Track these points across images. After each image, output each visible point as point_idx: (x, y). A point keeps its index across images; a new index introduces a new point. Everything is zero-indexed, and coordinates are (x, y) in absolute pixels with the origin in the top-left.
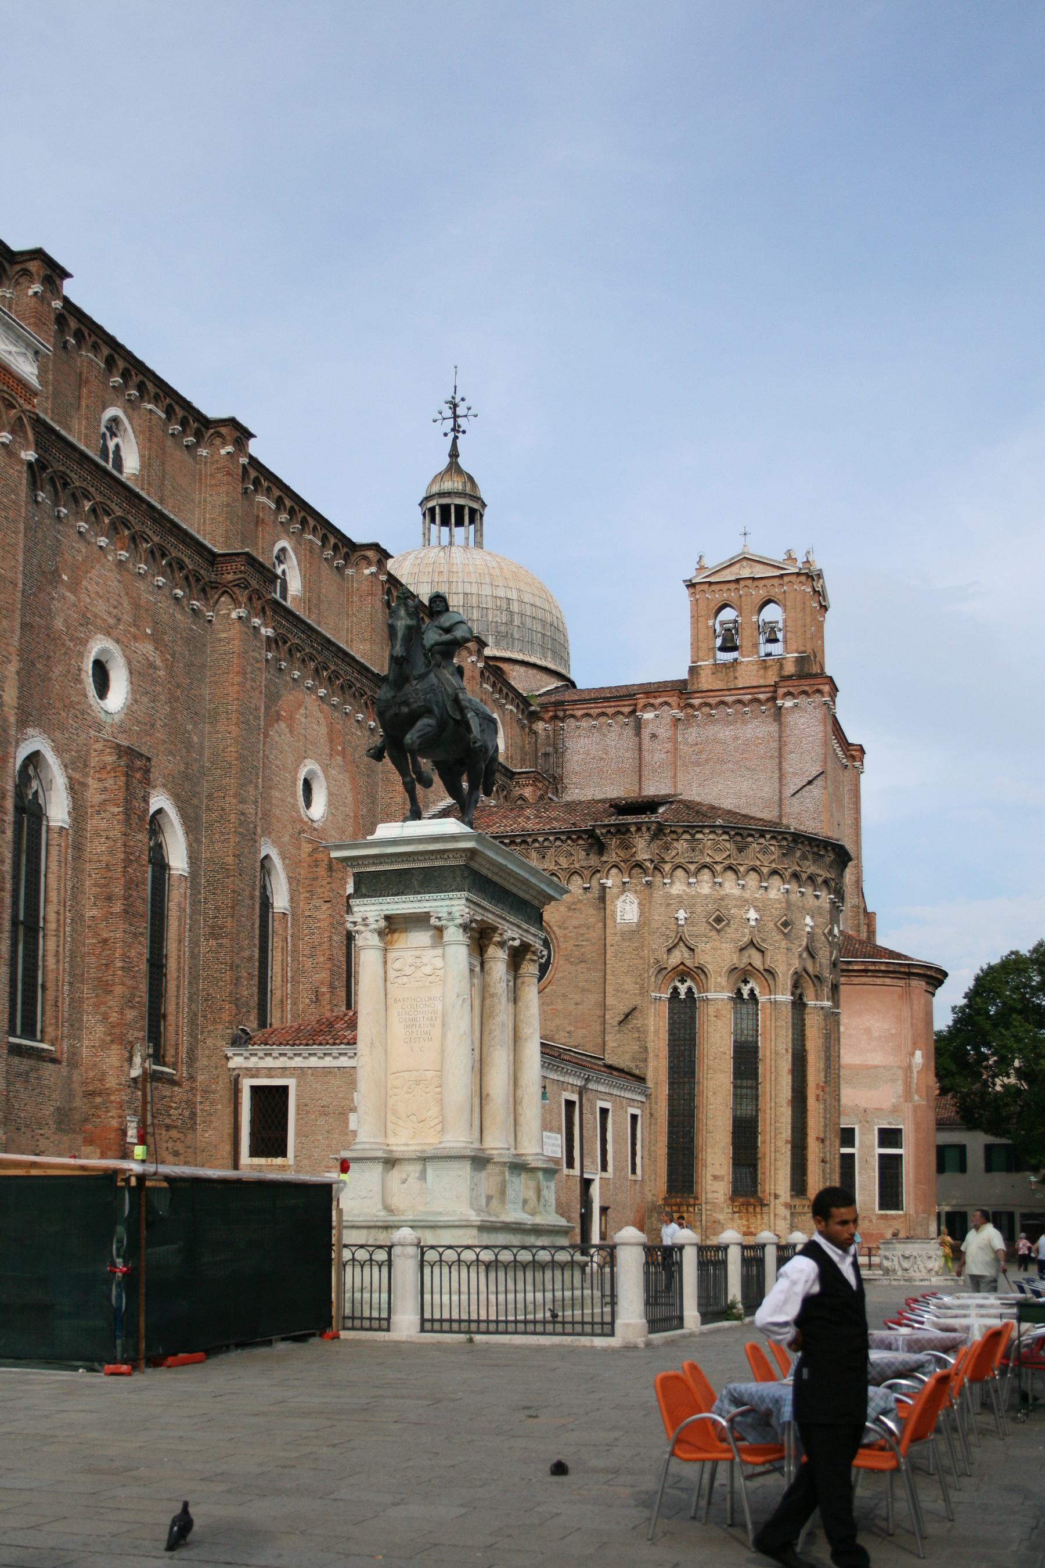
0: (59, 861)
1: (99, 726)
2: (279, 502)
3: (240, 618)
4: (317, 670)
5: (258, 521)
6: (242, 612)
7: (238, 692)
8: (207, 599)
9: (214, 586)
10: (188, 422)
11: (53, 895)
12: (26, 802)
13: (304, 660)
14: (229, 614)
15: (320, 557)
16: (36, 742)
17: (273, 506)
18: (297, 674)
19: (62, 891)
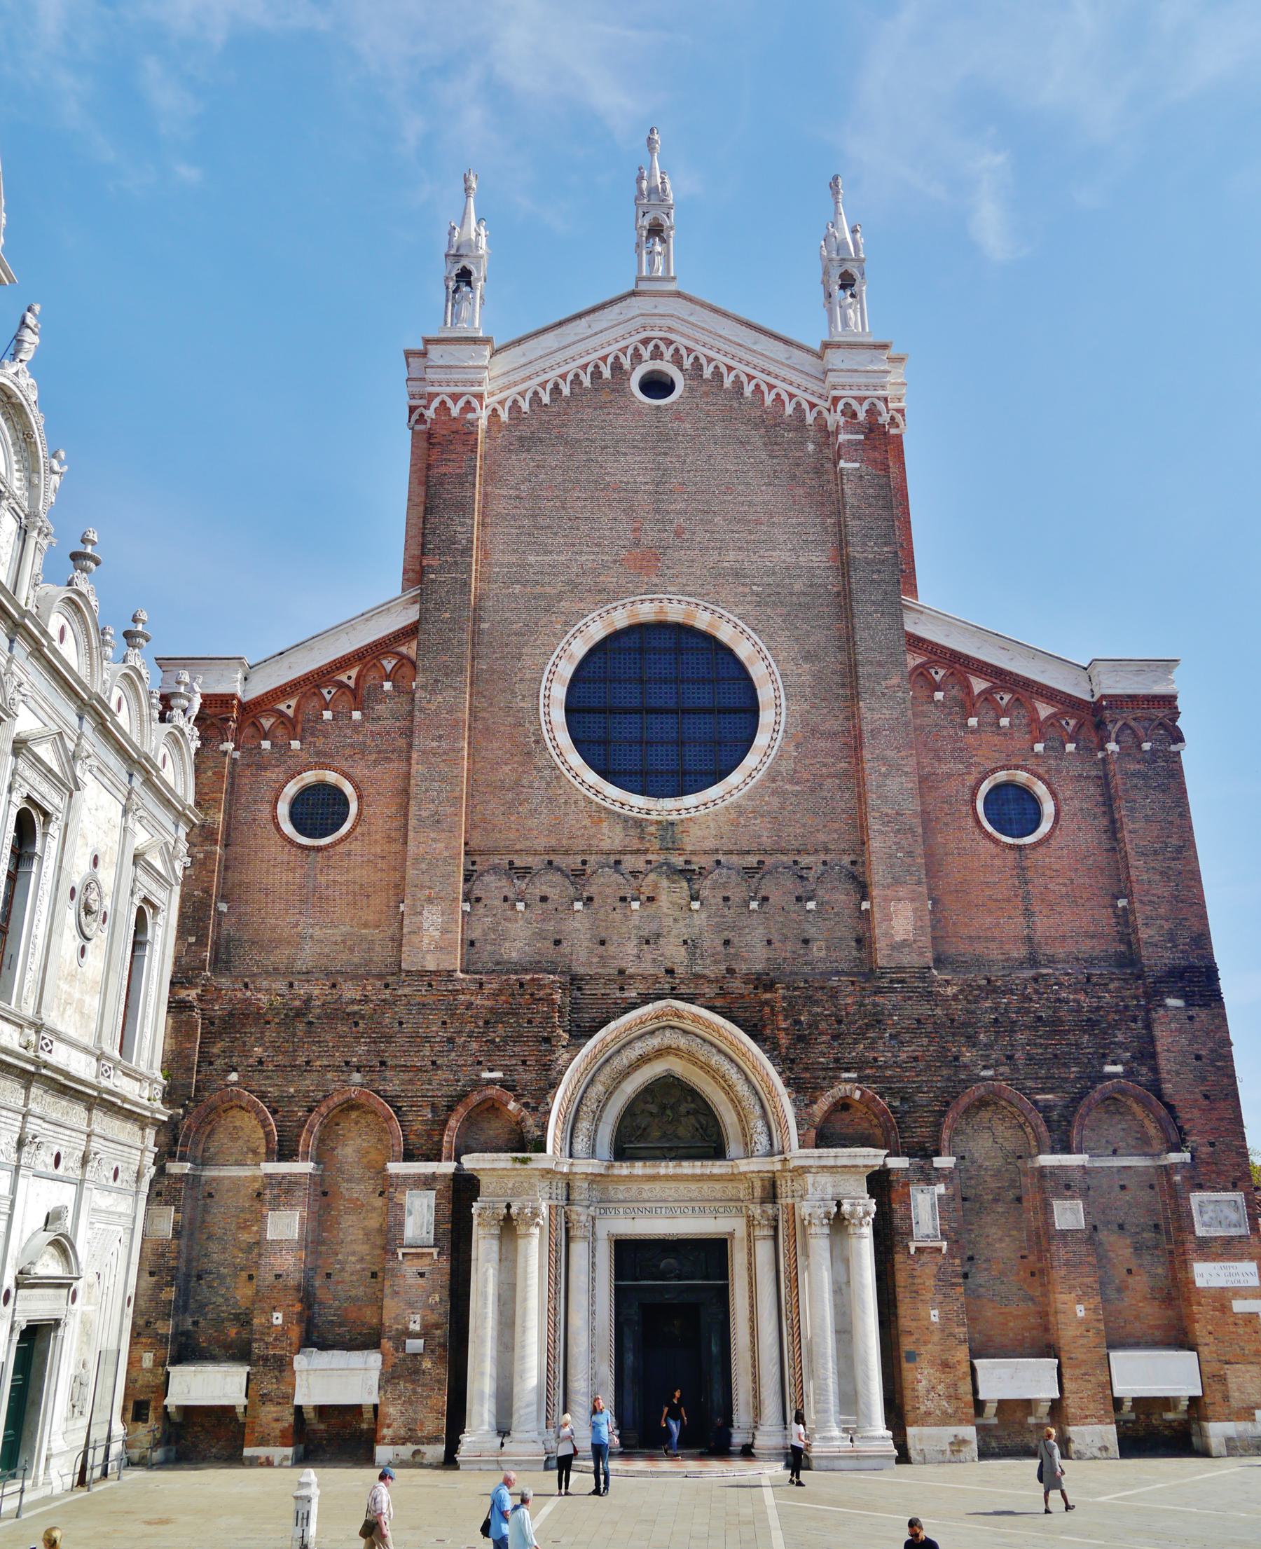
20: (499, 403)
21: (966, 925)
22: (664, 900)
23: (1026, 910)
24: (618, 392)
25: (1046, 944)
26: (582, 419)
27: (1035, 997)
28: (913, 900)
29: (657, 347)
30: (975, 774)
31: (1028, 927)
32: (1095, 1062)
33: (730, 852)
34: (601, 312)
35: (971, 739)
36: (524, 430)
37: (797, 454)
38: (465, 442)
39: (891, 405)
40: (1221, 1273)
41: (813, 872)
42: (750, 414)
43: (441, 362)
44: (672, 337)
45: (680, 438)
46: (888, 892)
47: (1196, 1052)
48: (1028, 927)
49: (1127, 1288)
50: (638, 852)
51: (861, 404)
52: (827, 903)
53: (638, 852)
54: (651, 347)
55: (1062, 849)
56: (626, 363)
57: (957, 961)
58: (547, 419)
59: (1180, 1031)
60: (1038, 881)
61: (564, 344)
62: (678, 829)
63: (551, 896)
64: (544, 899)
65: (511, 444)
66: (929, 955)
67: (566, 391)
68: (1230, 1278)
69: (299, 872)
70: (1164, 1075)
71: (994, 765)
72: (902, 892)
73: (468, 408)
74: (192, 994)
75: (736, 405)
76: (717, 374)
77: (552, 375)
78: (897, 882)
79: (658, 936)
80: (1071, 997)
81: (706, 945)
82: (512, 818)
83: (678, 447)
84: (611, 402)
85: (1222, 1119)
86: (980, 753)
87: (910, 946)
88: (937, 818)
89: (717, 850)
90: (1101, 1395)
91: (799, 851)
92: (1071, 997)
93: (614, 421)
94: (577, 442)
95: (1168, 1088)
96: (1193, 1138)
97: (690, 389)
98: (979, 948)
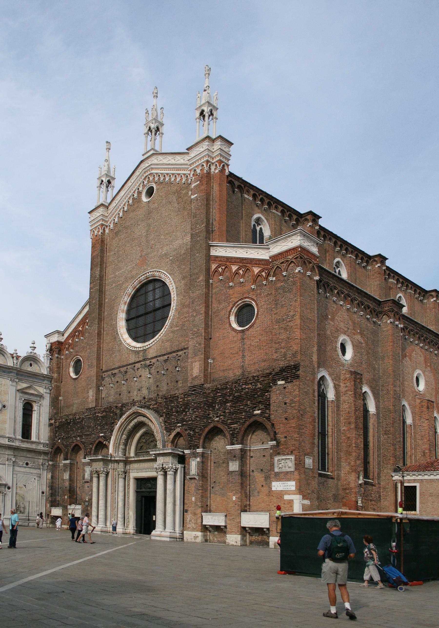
0: (332, 412)
1: (343, 365)
2: (398, 280)
3: (391, 322)
4: (419, 337)
5: (390, 288)
6: (392, 320)
7: (392, 348)
8: (378, 317)
9: (381, 313)
10: (363, 258)
11: (330, 423)
12: (320, 393)
13: (414, 335)
14: (387, 322)
15: (414, 298)
16: (323, 373)
17: (395, 282)
18: (412, 340)
19: (333, 422)
21: (223, 366)
22: (143, 377)
23: (243, 355)
25: (248, 367)
27: (234, 389)
28: (200, 361)
30: (231, 306)
31: (243, 362)
32: (251, 411)
33: (160, 356)
35: (231, 292)
40: (282, 485)
41: (181, 357)
46: (193, 360)
47: (285, 401)
48: (243, 362)
49: (261, 492)
50: (138, 362)
52: (183, 367)
53: (138, 362)
55: (258, 327)
57: (219, 380)
59: (280, 394)
60: (247, 342)
62: (147, 352)
63: (119, 381)
64: (117, 382)
66: (203, 380)
68: (284, 487)
69: (73, 386)
70: (272, 412)
71: (238, 300)
72: (197, 358)
74: (53, 421)
78: (196, 355)
79: (141, 388)
80: (247, 387)
81: (152, 389)
82: (111, 359)
85: (291, 427)
86: (234, 296)
87: (197, 378)
88: (217, 327)
89: (157, 356)
90: (237, 526)
91: (178, 351)
92: (247, 387)
95: (272, 417)
96: (279, 436)
98: (226, 374)
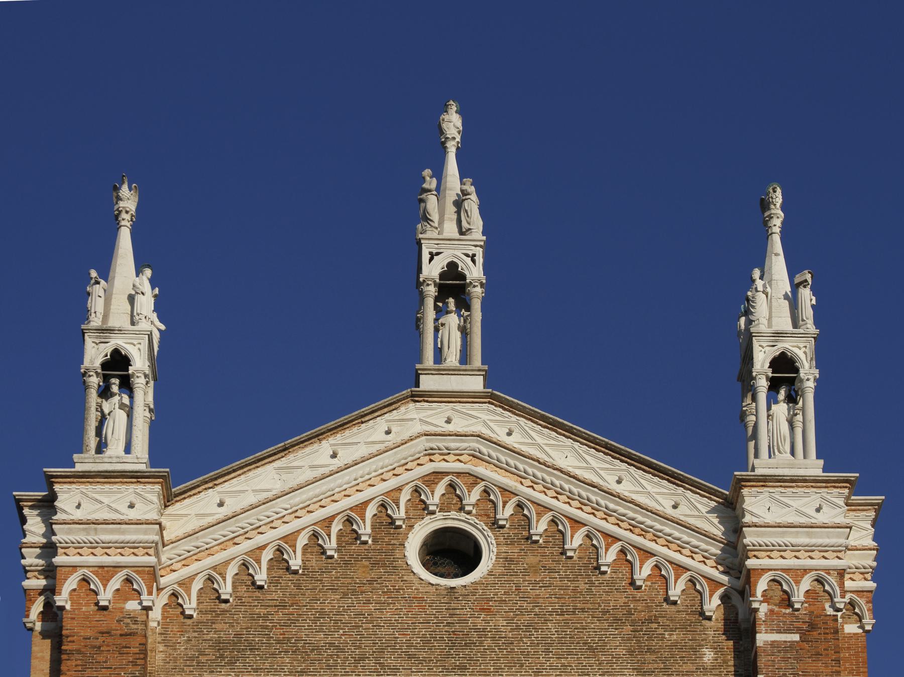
20: (181, 584)
24: (384, 566)
26: (322, 613)
29: (452, 486)
34: (355, 429)
36: (224, 630)
37: (685, 668)
38: (122, 650)
39: (848, 584)
42: (607, 602)
43: (78, 515)
44: (481, 470)
45: (488, 642)
51: (798, 583)
54: (441, 488)
56: (400, 514)
58: (263, 611)
61: (293, 484)
65: (202, 653)
67: (296, 563)
73: (129, 589)
75: (583, 586)
76: (557, 535)
77: (271, 535)
83: (484, 656)
84: (371, 582)
93: (377, 614)
94: (316, 649)
97: (506, 561)
